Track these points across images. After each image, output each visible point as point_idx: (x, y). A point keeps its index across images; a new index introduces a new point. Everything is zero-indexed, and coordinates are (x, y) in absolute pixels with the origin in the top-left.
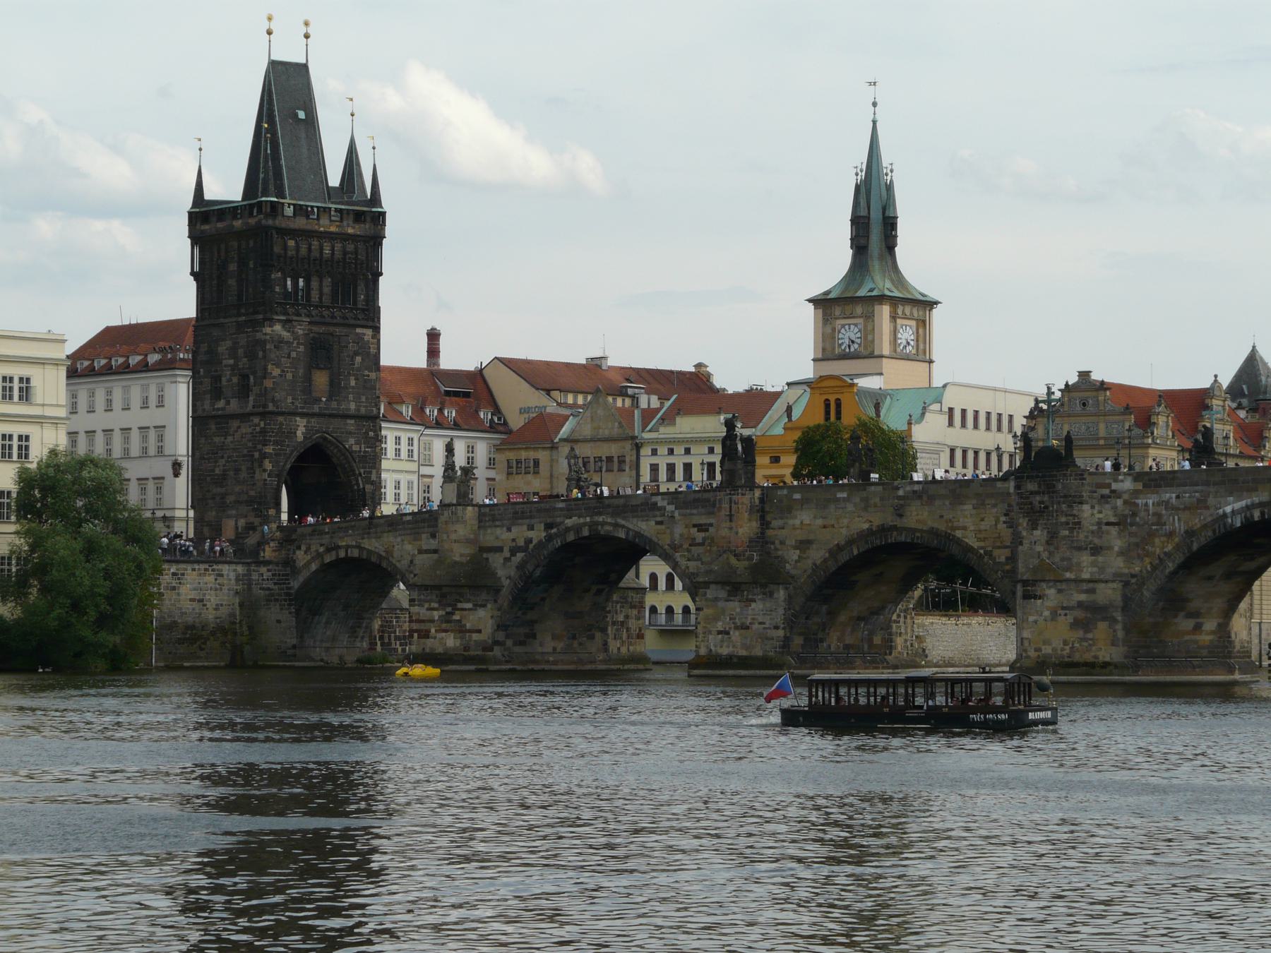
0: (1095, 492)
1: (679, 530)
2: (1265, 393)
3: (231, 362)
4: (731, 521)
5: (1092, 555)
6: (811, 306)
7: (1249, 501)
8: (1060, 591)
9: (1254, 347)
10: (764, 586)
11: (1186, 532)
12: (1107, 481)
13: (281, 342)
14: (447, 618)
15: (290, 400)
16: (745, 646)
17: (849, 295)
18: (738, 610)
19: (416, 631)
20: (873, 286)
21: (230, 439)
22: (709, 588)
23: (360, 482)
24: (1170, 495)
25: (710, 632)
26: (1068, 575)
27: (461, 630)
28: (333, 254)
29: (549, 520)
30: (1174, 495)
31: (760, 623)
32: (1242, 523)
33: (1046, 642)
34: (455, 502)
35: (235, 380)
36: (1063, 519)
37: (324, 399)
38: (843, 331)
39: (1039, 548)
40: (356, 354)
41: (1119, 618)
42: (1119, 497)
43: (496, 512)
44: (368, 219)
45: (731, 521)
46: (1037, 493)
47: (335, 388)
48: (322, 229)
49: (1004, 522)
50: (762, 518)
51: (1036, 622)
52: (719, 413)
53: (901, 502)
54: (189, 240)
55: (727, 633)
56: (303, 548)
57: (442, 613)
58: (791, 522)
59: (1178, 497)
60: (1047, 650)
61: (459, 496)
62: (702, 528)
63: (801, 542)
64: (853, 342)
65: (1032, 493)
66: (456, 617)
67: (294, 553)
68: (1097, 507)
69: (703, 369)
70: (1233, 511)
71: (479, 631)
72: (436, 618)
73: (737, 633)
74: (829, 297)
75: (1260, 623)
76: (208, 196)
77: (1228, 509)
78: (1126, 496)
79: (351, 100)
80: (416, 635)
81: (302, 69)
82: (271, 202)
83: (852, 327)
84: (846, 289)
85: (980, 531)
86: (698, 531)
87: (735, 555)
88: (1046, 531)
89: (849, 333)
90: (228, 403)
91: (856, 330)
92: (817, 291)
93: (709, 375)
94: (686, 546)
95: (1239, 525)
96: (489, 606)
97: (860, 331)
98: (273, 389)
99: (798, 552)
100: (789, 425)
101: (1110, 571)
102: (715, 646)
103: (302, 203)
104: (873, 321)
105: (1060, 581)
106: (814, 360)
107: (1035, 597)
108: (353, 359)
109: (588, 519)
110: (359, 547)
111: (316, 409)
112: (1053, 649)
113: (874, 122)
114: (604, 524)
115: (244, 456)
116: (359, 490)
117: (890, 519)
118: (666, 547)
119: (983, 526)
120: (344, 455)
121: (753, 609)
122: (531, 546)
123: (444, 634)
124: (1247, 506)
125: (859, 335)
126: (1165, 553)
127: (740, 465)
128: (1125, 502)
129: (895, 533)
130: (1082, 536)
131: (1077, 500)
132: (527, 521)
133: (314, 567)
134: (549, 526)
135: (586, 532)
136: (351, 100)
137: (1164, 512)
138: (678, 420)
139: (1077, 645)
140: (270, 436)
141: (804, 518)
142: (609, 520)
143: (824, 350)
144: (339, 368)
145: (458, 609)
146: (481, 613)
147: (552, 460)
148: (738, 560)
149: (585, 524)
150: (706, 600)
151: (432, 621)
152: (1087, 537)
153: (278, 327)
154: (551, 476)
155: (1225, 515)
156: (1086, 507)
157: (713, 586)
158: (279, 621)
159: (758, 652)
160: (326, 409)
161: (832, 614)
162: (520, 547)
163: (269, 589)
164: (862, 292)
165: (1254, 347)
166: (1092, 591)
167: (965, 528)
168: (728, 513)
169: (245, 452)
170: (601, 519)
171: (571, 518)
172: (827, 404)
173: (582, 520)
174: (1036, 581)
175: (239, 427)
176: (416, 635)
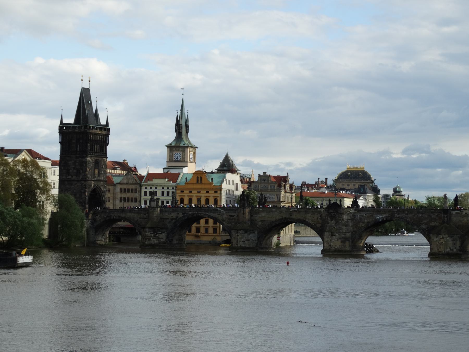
0: (346, 213)
1: (224, 216)
2: (232, 166)
3: (74, 166)
4: (244, 215)
5: (346, 226)
6: (166, 147)
7: (383, 216)
8: (339, 234)
9: (227, 153)
10: (253, 230)
11: (368, 222)
12: (349, 210)
13: (89, 162)
14: (155, 235)
15: (91, 177)
16: (249, 245)
17: (178, 145)
18: (247, 236)
19: (147, 239)
20: (184, 143)
21: (73, 186)
22: (240, 231)
23: (103, 198)
24: (364, 214)
25: (241, 241)
26: (341, 231)
27: (158, 239)
28: (99, 139)
29: (184, 212)
30: (365, 214)
31: (252, 239)
32: (381, 221)
33: (336, 246)
34: (155, 206)
35: (75, 171)
36: (340, 219)
37: (97, 177)
38: (175, 154)
39: (333, 225)
40: (103, 165)
41: (351, 240)
42: (351, 214)
43: (166, 209)
44: (106, 130)
45: (244, 215)
46: (333, 213)
47: (99, 174)
48: (98, 133)
49: (320, 218)
50: (251, 214)
51: (334, 241)
52: (166, 179)
53: (291, 212)
54: (59, 134)
55: (245, 242)
56: (99, 216)
57: (153, 234)
58: (259, 216)
59: (366, 214)
60: (336, 247)
61: (156, 205)
62: (231, 216)
63: (262, 220)
64: (178, 158)
65: (332, 212)
66: (157, 235)
67: (95, 217)
68: (347, 216)
69: (126, 161)
70: (379, 218)
71: (163, 239)
72: (152, 235)
73: (247, 241)
74: (172, 145)
75: (291, 234)
76: (64, 121)
77: (378, 218)
78: (353, 214)
79: (97, 97)
80: (147, 240)
81: (88, 89)
82: (89, 126)
83: (178, 154)
84: (176, 143)
85: (313, 220)
86: (231, 216)
87: (245, 223)
88: (335, 221)
89: (178, 155)
90: (72, 177)
91: (180, 154)
92: (168, 143)
93: (127, 163)
94: (227, 220)
95: (380, 221)
96: (165, 233)
97: (181, 155)
98: (88, 174)
99: (261, 223)
100: (186, 183)
101: (349, 230)
102: (242, 245)
103: (94, 126)
104: (185, 152)
105: (339, 232)
106: (167, 162)
107: (334, 236)
108: (103, 166)
109: (196, 212)
110: (119, 216)
111: (96, 179)
112: (337, 247)
113: (183, 99)
114: (201, 214)
115: (78, 191)
116: (103, 200)
117: (288, 216)
118: (221, 220)
119: (314, 219)
120: (100, 191)
121: (250, 236)
122: (178, 218)
123: (154, 240)
124: (383, 217)
125: (180, 156)
126: (362, 226)
127: (246, 201)
128: (352, 215)
129: (289, 219)
130: (344, 222)
131: (343, 214)
132: (177, 212)
133: (102, 221)
134: (183, 214)
135: (195, 216)
136: (97, 97)
137: (362, 217)
138: (153, 180)
139: (342, 246)
140: (87, 186)
141: (263, 215)
142: (203, 213)
143: (170, 159)
144: (100, 168)
145: (158, 233)
146: (163, 234)
147: (114, 189)
148: (246, 224)
149: (195, 214)
150: (240, 234)
151: (151, 236)
152: (345, 223)
153: (89, 158)
154: (114, 193)
155: (377, 219)
156: (345, 216)
157: (241, 230)
158: (92, 234)
159: (251, 246)
160: (97, 179)
161: (265, 237)
162: (174, 218)
163: (90, 226)
164: (182, 145)
165: (227, 153)
166: (345, 235)
167: (309, 219)
168: (243, 213)
169: (79, 190)
170: (200, 212)
171: (191, 212)
172: (198, 177)
173: (194, 213)
174: (334, 232)
175: (76, 183)
176: (147, 240)
